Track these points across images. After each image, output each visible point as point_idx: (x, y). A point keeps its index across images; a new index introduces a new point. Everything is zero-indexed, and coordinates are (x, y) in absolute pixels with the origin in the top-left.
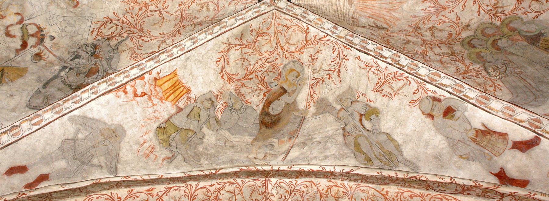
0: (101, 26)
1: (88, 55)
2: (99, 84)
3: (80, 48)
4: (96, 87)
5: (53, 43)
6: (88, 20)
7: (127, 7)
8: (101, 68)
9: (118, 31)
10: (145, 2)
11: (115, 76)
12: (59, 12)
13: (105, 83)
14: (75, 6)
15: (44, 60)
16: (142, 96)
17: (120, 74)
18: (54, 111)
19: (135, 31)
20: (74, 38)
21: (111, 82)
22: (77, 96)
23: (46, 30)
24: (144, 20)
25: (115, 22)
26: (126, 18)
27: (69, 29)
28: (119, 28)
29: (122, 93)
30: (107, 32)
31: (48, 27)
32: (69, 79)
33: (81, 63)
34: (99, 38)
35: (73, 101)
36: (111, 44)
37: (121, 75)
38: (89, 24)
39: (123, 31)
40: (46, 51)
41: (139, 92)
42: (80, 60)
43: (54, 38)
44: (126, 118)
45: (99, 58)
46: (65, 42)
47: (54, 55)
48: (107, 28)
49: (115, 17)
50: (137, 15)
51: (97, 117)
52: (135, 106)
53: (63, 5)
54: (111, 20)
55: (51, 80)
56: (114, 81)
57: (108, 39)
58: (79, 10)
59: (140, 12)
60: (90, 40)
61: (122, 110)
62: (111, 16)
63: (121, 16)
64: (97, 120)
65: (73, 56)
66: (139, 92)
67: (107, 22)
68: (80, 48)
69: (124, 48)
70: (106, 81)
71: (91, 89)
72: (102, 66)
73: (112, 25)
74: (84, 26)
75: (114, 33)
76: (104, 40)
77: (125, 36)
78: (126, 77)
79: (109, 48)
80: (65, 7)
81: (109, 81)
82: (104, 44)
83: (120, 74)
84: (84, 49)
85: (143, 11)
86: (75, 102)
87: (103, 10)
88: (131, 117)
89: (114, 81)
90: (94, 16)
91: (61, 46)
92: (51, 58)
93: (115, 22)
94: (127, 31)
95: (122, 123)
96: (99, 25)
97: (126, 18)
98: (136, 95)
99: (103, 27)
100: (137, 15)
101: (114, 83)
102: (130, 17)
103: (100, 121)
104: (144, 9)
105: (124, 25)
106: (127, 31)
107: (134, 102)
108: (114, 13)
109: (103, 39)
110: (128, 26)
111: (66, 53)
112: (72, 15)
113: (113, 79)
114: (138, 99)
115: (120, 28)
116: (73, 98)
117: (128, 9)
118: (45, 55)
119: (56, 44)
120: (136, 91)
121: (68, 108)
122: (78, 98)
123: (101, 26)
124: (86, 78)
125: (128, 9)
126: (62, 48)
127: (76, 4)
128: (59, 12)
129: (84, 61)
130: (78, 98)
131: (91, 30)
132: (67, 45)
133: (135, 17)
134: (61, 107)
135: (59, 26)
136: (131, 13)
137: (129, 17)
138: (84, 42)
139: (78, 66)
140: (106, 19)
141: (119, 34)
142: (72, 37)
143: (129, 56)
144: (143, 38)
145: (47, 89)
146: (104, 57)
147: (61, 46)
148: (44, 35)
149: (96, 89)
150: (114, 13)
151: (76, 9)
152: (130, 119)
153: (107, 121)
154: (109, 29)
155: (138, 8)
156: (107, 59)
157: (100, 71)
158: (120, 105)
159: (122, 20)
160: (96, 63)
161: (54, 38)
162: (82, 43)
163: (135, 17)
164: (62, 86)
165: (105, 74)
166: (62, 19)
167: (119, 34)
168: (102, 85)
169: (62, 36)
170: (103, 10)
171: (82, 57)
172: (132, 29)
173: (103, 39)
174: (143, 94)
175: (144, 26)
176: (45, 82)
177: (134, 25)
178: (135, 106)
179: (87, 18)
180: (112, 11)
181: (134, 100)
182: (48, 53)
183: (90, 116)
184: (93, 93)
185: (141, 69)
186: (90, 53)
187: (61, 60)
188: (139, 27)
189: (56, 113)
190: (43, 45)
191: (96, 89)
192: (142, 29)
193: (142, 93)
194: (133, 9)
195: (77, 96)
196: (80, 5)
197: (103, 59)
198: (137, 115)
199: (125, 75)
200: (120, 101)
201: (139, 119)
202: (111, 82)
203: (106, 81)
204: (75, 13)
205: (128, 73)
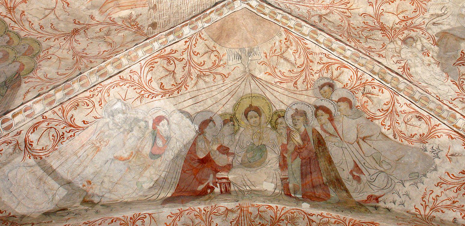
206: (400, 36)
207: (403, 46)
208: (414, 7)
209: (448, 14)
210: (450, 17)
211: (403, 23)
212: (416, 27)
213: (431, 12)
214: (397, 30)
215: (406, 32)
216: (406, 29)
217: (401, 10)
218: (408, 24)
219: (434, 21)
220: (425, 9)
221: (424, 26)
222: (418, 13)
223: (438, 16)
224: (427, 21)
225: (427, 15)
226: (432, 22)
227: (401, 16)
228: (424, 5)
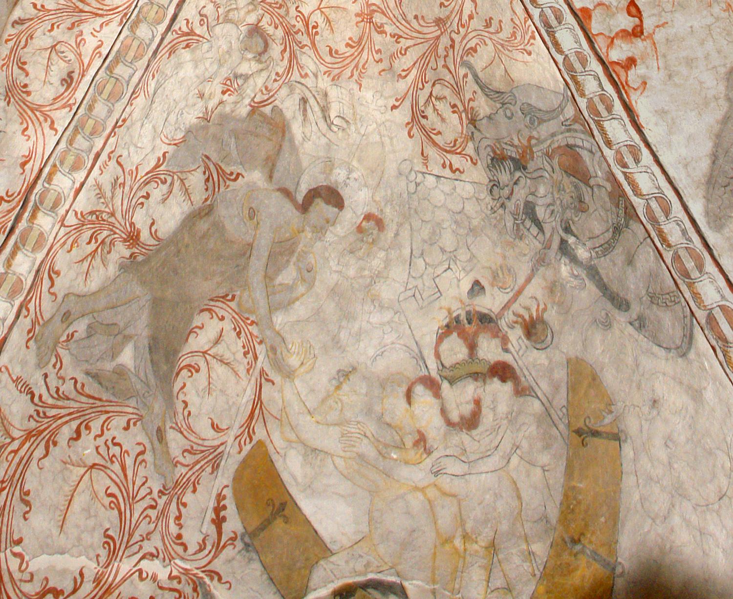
0: (435, 144)
1: (522, 181)
2: (609, 144)
3: (503, 206)
4: (618, 152)
5: (492, 285)
6: (417, 185)
7: (374, 69)
8: (560, 140)
9: (447, 92)
10: (357, 15)
11: (583, 95)
12: (398, 273)
13: (606, 125)
14: (380, 224)
15: (545, 310)
16: (639, 14)
17: (577, 83)
18: (695, 274)
19: (445, 41)
20: (475, 222)
21: (601, 108)
22: (648, 207)
23: (453, 308)
24: (410, 17)
25: (422, 102)
26: (409, 70)
27: (448, 240)
28: (438, 90)
29: (632, 73)
30: (452, 126)
31: (444, 302)
32: (597, 232)
33: (548, 200)
34: (470, 149)
35: (662, 218)
36: (488, 111)
37: (580, 78)
38: (431, 179)
39: (448, 77)
40: (516, 307)
41: (626, 22)
42: (540, 202)
43: (477, 283)
44: (707, 57)
45: (530, 147)
46: (487, 251)
47: (528, 280)
48: (439, 126)
49: (407, 103)
50: (397, 37)
51: (707, 146)
52: (671, 31)
53: (377, 263)
54: (417, 117)
55: (603, 287)
56: (596, 100)
57: (473, 121)
58: (389, 214)
59: (389, 29)
60: (478, 174)
61: (684, 70)
62: (403, 115)
63: (402, 86)
64: (717, 146)
65: (528, 223)
66: (626, 22)
67: (423, 128)
68: (503, 206)
69: (499, 72)
70: (598, 124)
71: (625, 166)
72: (553, 135)
73: (429, 112)
74: (438, 197)
75: (454, 106)
76: (477, 134)
77: (462, 71)
78: (584, 62)
79: (500, 117)
80: (382, 254)
81: (598, 114)
82: (489, 133)
83: (577, 83)
84: (506, 191)
85: (385, 20)
86: (667, 212)
87: (387, 140)
88: (702, 43)
89: (596, 100)
90: (405, 167)
91: (500, 261)
92: (536, 288)
93: (422, 102)
94: (445, 66)
95: (723, 70)
96: (431, 152)
97: (409, 70)
98: (637, 32)
99: (437, 139)
100: (397, 37)
101: (603, 98)
102: (403, 59)
103: (718, 136)
104: (378, 18)
105: (430, 75)
106: (445, 66)
107: (656, 37)
108: (394, 107)
109: (472, 138)
110: (432, 64)
111: (521, 244)
112: (405, 233)
113: (590, 100)
114: (649, 24)
115: (438, 86)
116: (654, 220)
117: (381, 66)
118: (528, 309)
119: (495, 276)
120: (624, 31)
121: (684, 232)
122: (654, 205)
123: (435, 144)
124: (592, 182)
125: (381, 66)
126: (504, 257)
127: (372, 223)
128: (398, 273)
129: (542, 190)
130: (654, 205)
131: (447, 172)
132: (494, 244)
133: (404, 43)
134: (682, 253)
135: (439, 271)
136: (391, 56)
137: (406, 62)
138: (484, 195)
139: (557, 208)
140: (414, 131)
141: (458, 90)
142: (472, 230)
143: (520, 56)
144: (465, 17)
145: (631, 297)
146: (526, 133)
147: (500, 261)
148: (468, 313)
149: (624, 150)
150: (394, 107)
151: (386, 221)
152: (709, 45)
153: (719, 114)
154: (443, 120)
155: (377, 38)
156: (532, 122)
157: (571, 141)
158: (670, 76)
159: (415, 82)
160: (547, 154)
161: (477, 283)
162: (489, 199)
163: (404, 43)
164: (618, 254)
165: (577, 126)
166: (420, 263)
167: (458, 90)
168: (610, 135)
169: (470, 260)
170: (387, 140)
171: (531, 198)
172: (441, 51)
173: (472, 138)
174: (633, 10)
175: (430, 17)
176: (609, 306)
177: (427, 45)
178: (671, 31)
179: (412, 187)
180: (389, 115)
181: (650, 36)
182: (521, 299)
183: (704, 165)
184: (637, 161)
185: (559, 19)
186: (518, 174)
187: (541, 261)
188: (432, 31)
189: (700, 267)
190: (500, 315)
191: (624, 150)
192: (439, 22)
193: (629, 14)
194: (379, 51)
195: (648, 207)
196: (375, 211)
197: (535, 134)
198: (696, 24)
199: (577, 66)
200: (656, 78)
201: (710, 20)
202: (601, 108)
203: (598, 124)
204: (400, 225)
205: (573, 59)
206: (267, 19)
207: (244, 29)
208: (342, 48)
209: (330, 135)
210: (324, 140)
211: (300, 25)
212: (293, 57)
213: (333, 93)
214: (282, 12)
215: (280, 33)
216: (288, 33)
217: (332, 16)
218: (299, 37)
219: (312, 101)
220: (339, 75)
221: (296, 76)
222: (328, 59)
223: (325, 110)
224: (310, 82)
225: (324, 83)
226: (308, 95)
227: (317, 18)
228: (348, 72)
